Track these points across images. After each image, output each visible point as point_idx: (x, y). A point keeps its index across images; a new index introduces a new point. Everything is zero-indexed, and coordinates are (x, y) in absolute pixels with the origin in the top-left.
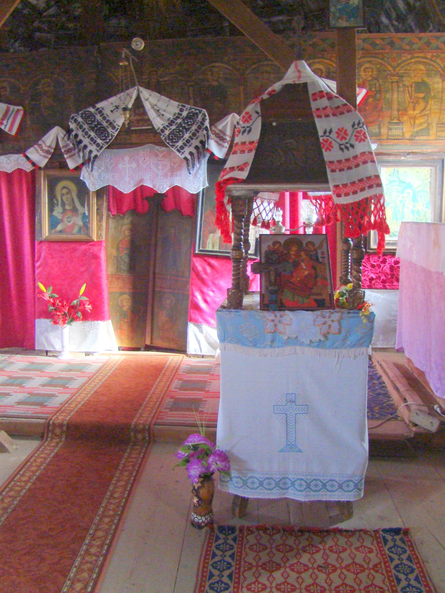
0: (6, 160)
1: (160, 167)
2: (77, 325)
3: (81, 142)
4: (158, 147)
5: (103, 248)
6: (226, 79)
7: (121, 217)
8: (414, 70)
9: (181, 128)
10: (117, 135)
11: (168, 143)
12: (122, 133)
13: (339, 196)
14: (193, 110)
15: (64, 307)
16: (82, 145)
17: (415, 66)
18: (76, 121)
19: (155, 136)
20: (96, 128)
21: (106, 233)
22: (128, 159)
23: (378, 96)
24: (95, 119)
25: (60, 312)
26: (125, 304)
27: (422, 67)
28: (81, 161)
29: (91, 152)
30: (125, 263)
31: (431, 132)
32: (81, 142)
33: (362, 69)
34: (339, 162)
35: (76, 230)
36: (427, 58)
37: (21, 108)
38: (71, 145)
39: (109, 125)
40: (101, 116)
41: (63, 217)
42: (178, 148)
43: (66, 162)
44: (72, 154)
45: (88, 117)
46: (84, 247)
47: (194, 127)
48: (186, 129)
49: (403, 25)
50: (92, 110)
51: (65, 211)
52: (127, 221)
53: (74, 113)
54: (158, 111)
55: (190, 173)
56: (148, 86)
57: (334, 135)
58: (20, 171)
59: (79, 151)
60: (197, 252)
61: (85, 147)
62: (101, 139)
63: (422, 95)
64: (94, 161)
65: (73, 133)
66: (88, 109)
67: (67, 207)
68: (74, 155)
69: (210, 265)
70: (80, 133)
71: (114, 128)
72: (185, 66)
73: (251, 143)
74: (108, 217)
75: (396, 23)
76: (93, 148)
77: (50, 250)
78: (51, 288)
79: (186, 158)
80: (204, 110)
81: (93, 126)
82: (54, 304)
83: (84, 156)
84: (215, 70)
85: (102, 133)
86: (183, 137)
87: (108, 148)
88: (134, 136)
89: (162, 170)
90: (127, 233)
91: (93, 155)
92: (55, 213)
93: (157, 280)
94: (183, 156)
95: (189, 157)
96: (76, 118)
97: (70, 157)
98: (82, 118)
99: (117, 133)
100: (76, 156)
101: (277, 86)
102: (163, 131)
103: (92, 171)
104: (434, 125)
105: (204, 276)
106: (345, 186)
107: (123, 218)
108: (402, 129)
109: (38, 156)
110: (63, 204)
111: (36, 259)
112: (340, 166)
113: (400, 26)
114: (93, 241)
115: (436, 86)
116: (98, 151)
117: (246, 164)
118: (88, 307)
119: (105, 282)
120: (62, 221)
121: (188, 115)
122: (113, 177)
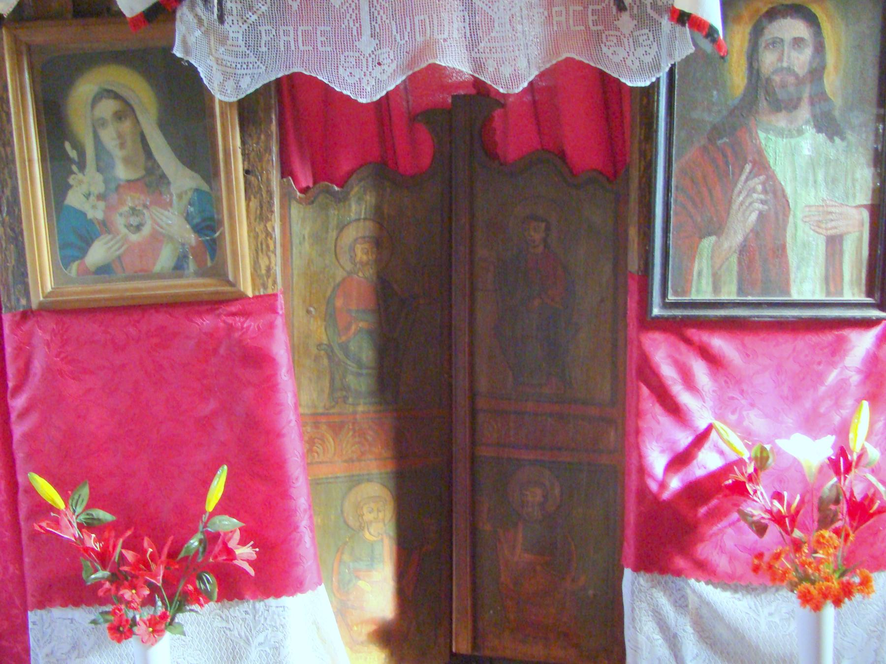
2: (202, 622)
5: (279, 321)
7: (333, 194)
15: (148, 567)
21: (296, 263)
25: (133, 586)
26: (368, 517)
30: (359, 363)
35: (165, 259)
41: (109, 209)
46: (207, 322)
52: (358, 208)
60: (656, 311)
74: (286, 197)
77: (65, 343)
78: (85, 492)
82: (103, 558)
90: (362, 253)
92: (74, 199)
93: (481, 417)
103: (221, 19)
105: (685, 398)
107: (341, 199)
111: (11, 384)
114: (241, 297)
118: (245, 553)
119: (293, 446)
120: (106, 226)
122: (308, 37)
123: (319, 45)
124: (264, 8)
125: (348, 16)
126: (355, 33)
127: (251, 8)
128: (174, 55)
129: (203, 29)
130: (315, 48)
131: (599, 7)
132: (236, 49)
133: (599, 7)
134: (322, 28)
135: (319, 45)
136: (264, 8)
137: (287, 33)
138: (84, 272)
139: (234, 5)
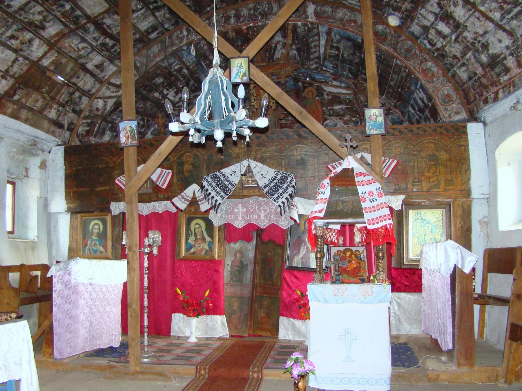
0: (158, 204)
1: (262, 211)
3: (210, 194)
6: (306, 155)
8: (427, 148)
13: (370, 224)
16: (211, 196)
17: (427, 145)
18: (207, 180)
19: (259, 191)
23: (405, 164)
27: (432, 145)
28: (209, 207)
29: (216, 201)
31: (441, 186)
32: (210, 194)
33: (394, 147)
34: (370, 208)
36: (435, 140)
37: (170, 171)
41: (195, 243)
48: (280, 187)
49: (423, 114)
50: (218, 174)
51: (196, 239)
56: (255, 159)
57: (367, 194)
58: (168, 212)
61: (213, 197)
63: (433, 163)
64: (218, 207)
65: (205, 188)
67: (198, 237)
69: (295, 277)
70: (210, 189)
71: (232, 185)
72: (279, 147)
73: (325, 199)
75: (419, 113)
76: (218, 198)
79: (279, 206)
83: (212, 203)
84: (298, 149)
85: (225, 189)
87: (227, 198)
88: (246, 190)
89: (264, 213)
91: (218, 203)
92: (189, 241)
94: (277, 204)
95: (282, 205)
101: (339, 170)
102: (265, 188)
104: (442, 182)
105: (291, 284)
106: (373, 220)
108: (421, 185)
109: (181, 203)
110: (196, 235)
112: (370, 210)
113: (421, 115)
115: (442, 157)
117: (323, 209)
120: (194, 246)
138: (190, 253)
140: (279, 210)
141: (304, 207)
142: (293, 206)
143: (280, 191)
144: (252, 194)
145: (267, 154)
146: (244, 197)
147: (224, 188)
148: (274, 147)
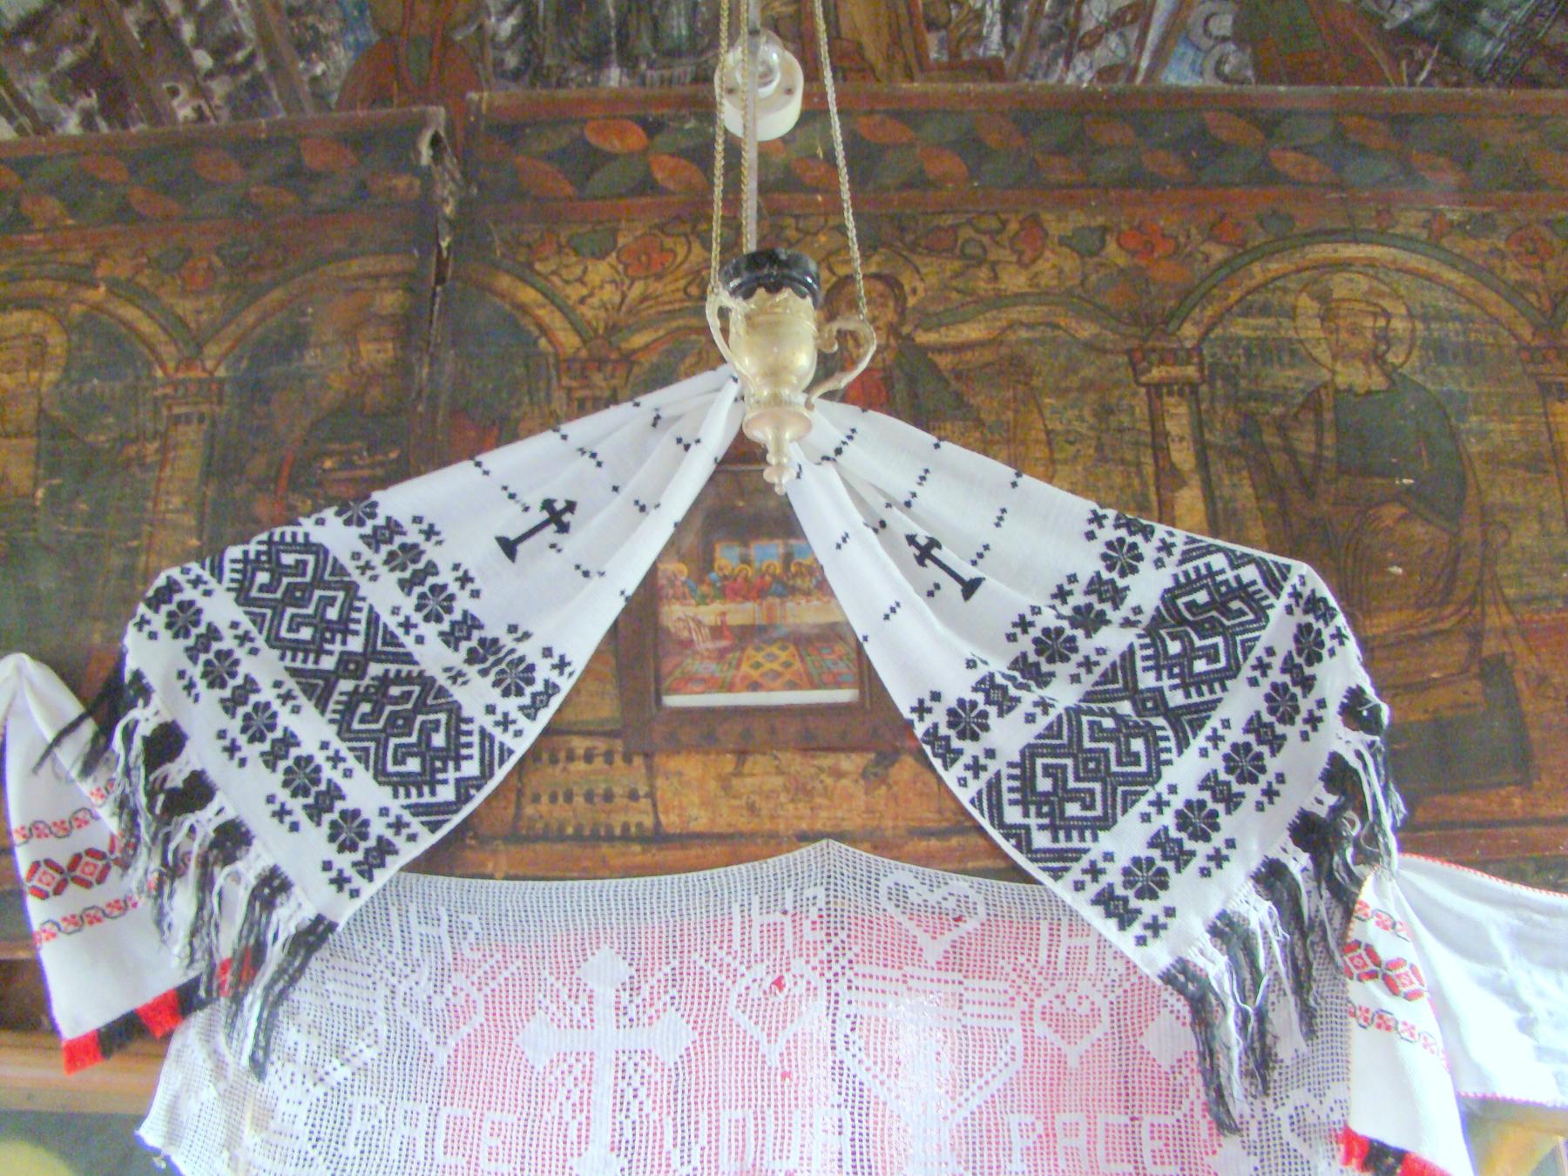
3: (198, 791)
4: (903, 874)
6: (1439, 351)
9: (1125, 708)
10: (533, 754)
11: (1021, 836)
12: (580, 744)
14: (1218, 561)
16: (206, 820)
18: (184, 620)
19: (874, 776)
20: (346, 685)
22: (624, 970)
24: (349, 607)
28: (168, 970)
29: (273, 887)
32: (198, 791)
38: (110, 823)
39: (472, 658)
40: (406, 586)
42: (1113, 875)
43: (35, 969)
44: (99, 896)
45: (296, 596)
47: (1240, 703)
50: (336, 535)
53: (180, 560)
54: (925, 552)
55: (1224, 1124)
59: (172, 870)
61: (232, 839)
62: (381, 775)
64: (291, 975)
65: (145, 718)
66: (307, 525)
68: (122, 906)
70: (204, 719)
71: (514, 678)
76: (301, 851)
79: (1182, 978)
80: (1300, 568)
81: (328, 663)
86: (1152, 777)
87: (428, 864)
88: (690, 766)
91: (288, 918)
94: (1157, 957)
95: (1215, 966)
96: (189, 594)
97: (80, 921)
98: (242, 595)
99: (532, 730)
100: (135, 928)
102: (967, 721)
103: (258, 1067)
116: (340, 881)
121: (1169, 597)
123: (484, 1156)
124: (369, 1054)
125: (562, 1096)
126: (573, 1134)
127: (339, 1050)
128: (139, 1142)
129: (222, 1085)
130: (473, 1162)
131: (1170, 1120)
132: (286, 1142)
133: (1170, 1120)
134: (497, 1116)
135: (484, 1156)
136: (369, 1054)
137: (411, 1118)
139: (302, 1039)
140: (1167, 1035)
141: (1509, 995)
142: (1385, 974)
143: (1186, 771)
144: (793, 815)
145: (972, 332)
146: (667, 848)
147: (392, 709)
148: (1055, 265)
